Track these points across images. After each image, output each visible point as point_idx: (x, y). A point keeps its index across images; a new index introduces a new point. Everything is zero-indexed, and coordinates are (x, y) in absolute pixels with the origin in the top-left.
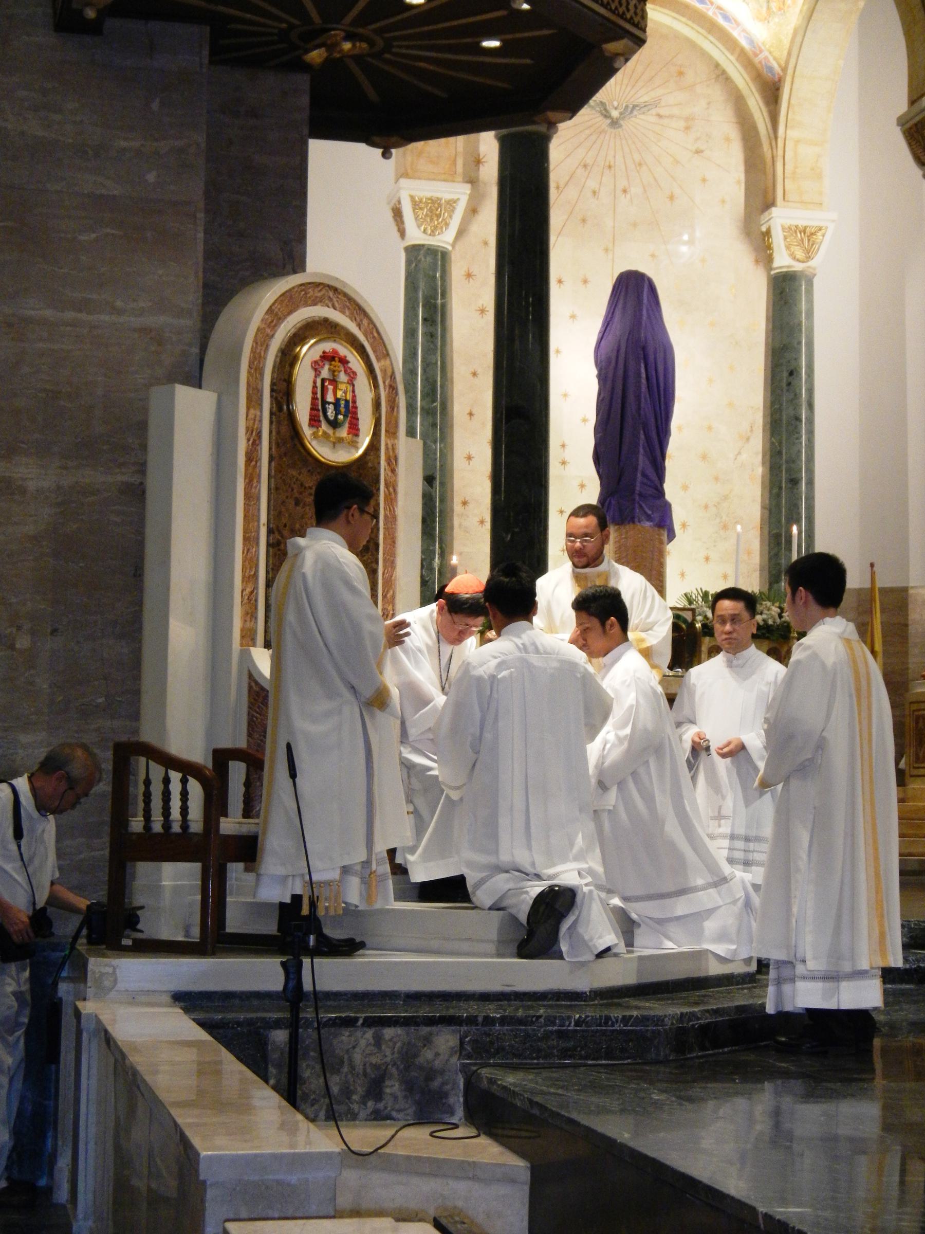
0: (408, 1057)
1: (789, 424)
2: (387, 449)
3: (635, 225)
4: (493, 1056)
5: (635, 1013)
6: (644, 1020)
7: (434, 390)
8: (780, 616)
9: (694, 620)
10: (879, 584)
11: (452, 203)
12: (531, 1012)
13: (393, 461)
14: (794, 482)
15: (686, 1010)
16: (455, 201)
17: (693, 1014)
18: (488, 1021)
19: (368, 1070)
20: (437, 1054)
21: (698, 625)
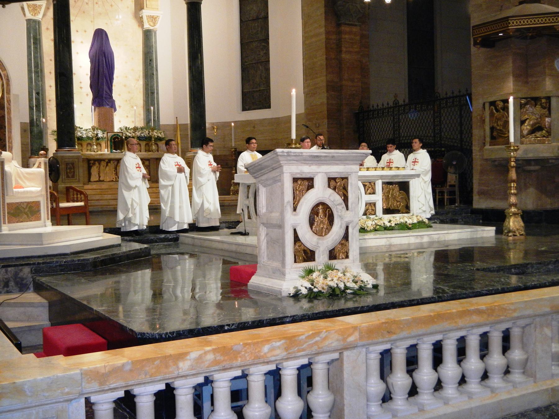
0: (16, 274)
1: (150, 76)
2: (7, 98)
3: (100, 14)
4: (41, 273)
5: (82, 258)
6: (84, 260)
7: (38, 65)
8: (149, 134)
9: (123, 135)
10: (179, 123)
11: (40, 6)
12: (52, 260)
13: (9, 101)
14: (153, 93)
15: (97, 256)
16: (42, 5)
17: (98, 257)
18: (39, 264)
19: (4, 279)
20: (24, 274)
21: (124, 137)
